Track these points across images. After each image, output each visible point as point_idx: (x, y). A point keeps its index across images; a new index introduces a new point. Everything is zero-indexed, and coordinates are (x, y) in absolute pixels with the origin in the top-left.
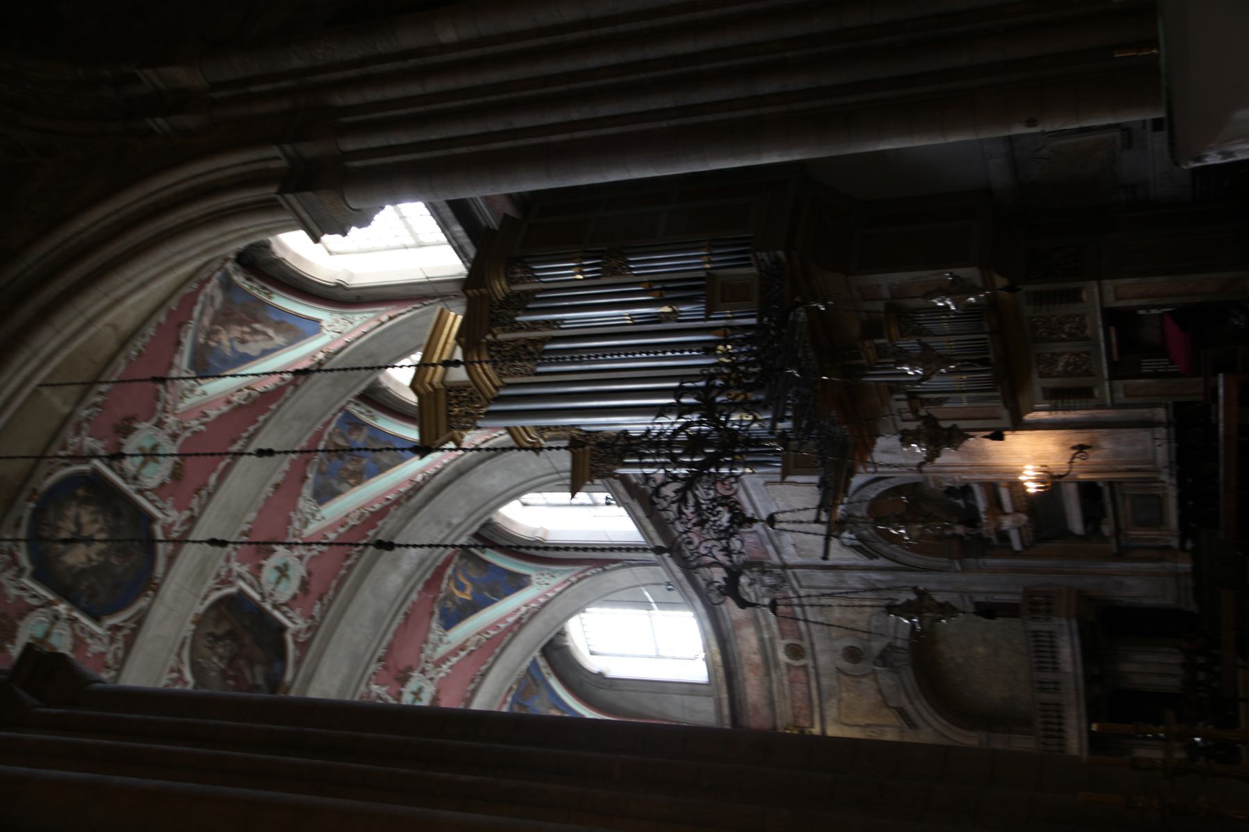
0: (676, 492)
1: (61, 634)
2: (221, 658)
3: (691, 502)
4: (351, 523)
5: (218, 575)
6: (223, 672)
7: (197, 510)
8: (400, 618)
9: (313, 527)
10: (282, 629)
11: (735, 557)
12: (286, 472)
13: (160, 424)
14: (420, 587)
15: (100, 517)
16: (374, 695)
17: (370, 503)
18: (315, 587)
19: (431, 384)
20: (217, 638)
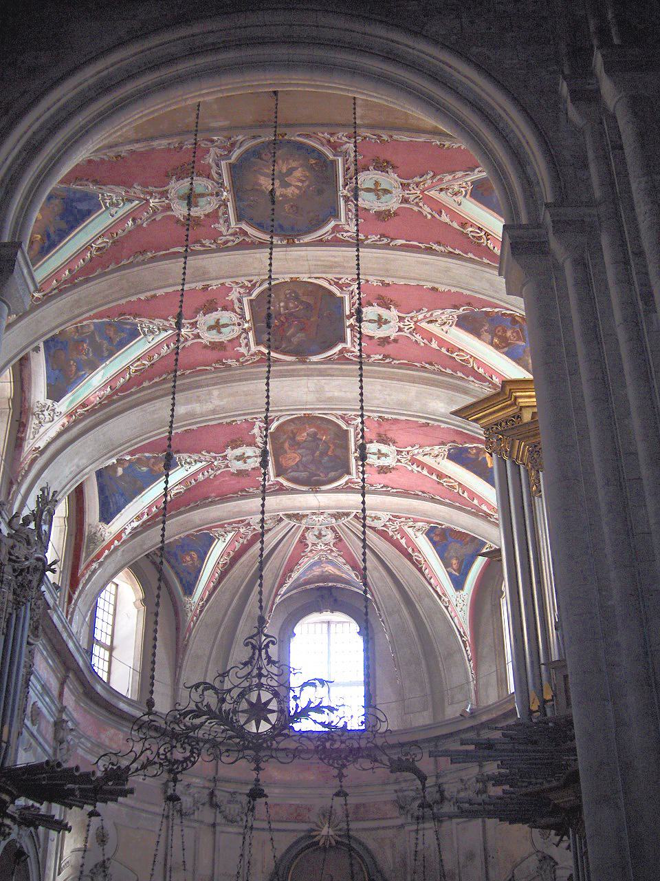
0: (208, 706)
1: (210, 203)
2: (286, 308)
3: (197, 721)
4: (454, 355)
5: (340, 279)
6: (280, 314)
7: (369, 241)
8: (424, 421)
9: (433, 328)
10: (344, 340)
11: (141, 772)
12: (449, 291)
13: (404, 186)
14: (453, 427)
15: (307, 183)
16: (353, 422)
17: (481, 364)
18: (389, 349)
19: (516, 398)
20: (297, 298)
